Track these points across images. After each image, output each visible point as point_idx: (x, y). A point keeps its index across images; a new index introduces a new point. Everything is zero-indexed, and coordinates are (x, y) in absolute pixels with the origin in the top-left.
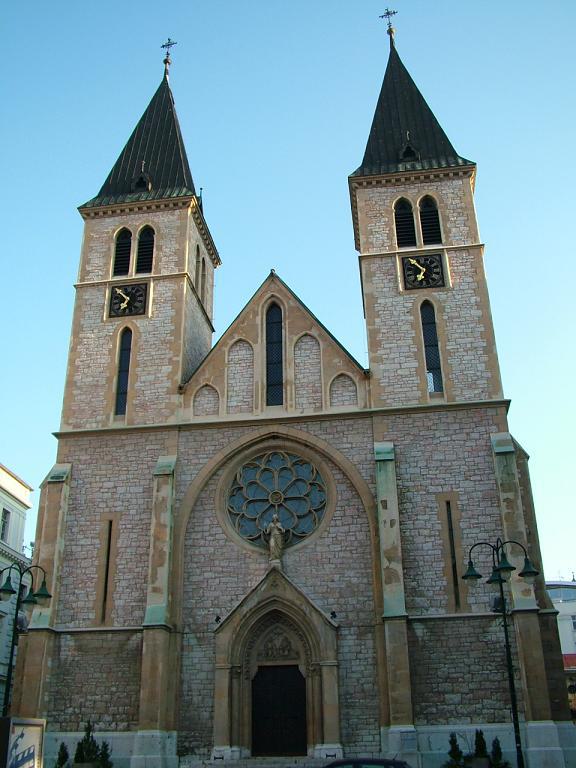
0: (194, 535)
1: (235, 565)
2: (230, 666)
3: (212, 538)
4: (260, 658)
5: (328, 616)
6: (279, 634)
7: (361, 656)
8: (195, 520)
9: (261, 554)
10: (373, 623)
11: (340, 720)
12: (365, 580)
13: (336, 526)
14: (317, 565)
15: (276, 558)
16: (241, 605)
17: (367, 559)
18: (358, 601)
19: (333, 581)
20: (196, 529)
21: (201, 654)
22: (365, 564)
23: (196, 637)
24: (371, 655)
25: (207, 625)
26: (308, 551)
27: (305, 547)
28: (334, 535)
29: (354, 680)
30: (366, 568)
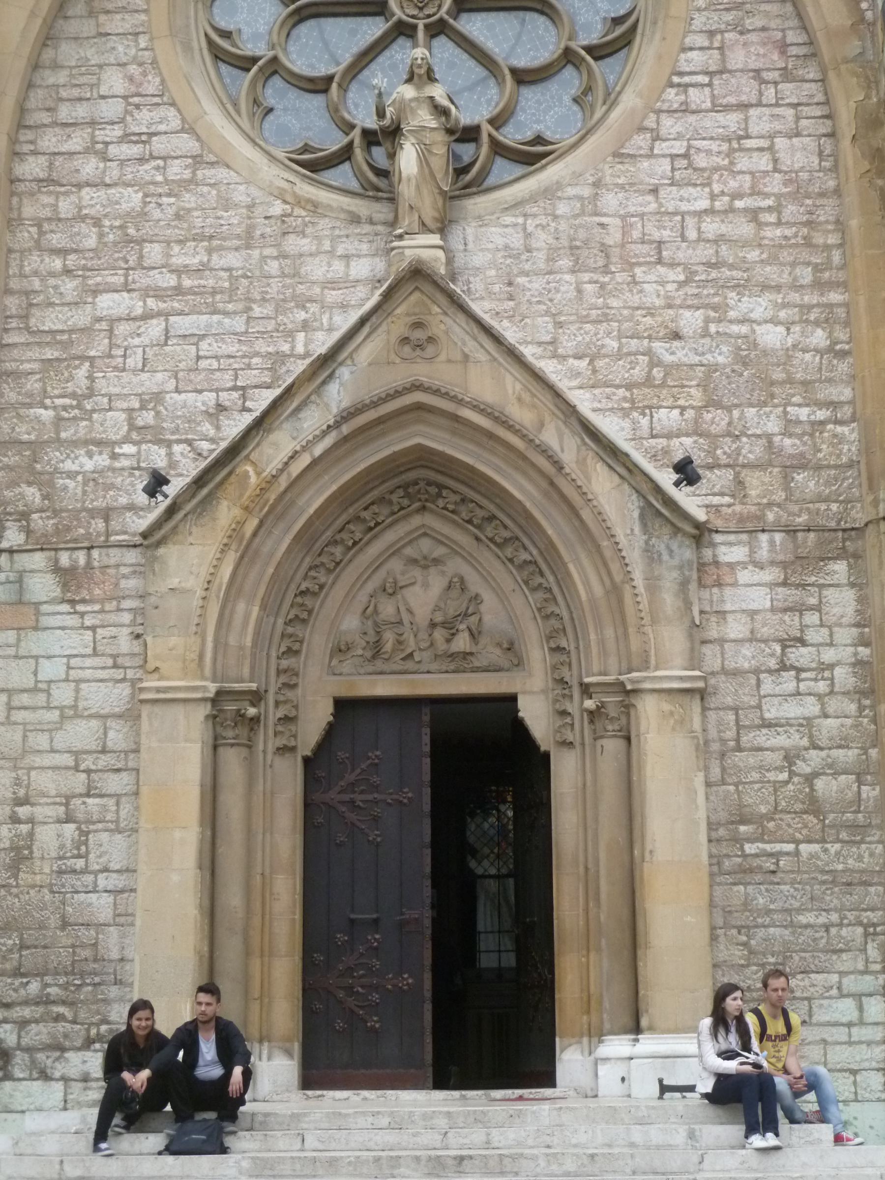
0: (49, 141)
1: (233, 260)
2: (212, 688)
3: (135, 150)
4: (347, 667)
5: (666, 478)
6: (426, 563)
7: (800, 655)
8: (61, 77)
9: (355, 219)
10: (859, 516)
11: (714, 938)
12: (819, 337)
13: (686, 109)
14: (606, 270)
15: (425, 228)
16: (260, 424)
17: (827, 248)
18: (789, 425)
19: (677, 336)
20: (64, 113)
21: (80, 642)
22: (817, 268)
23: (57, 569)
24: (846, 654)
25: (107, 514)
26: (562, 209)
27: (550, 193)
28: (679, 147)
29: (776, 758)
30: (819, 285)
